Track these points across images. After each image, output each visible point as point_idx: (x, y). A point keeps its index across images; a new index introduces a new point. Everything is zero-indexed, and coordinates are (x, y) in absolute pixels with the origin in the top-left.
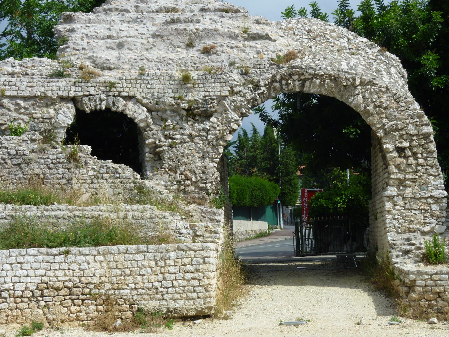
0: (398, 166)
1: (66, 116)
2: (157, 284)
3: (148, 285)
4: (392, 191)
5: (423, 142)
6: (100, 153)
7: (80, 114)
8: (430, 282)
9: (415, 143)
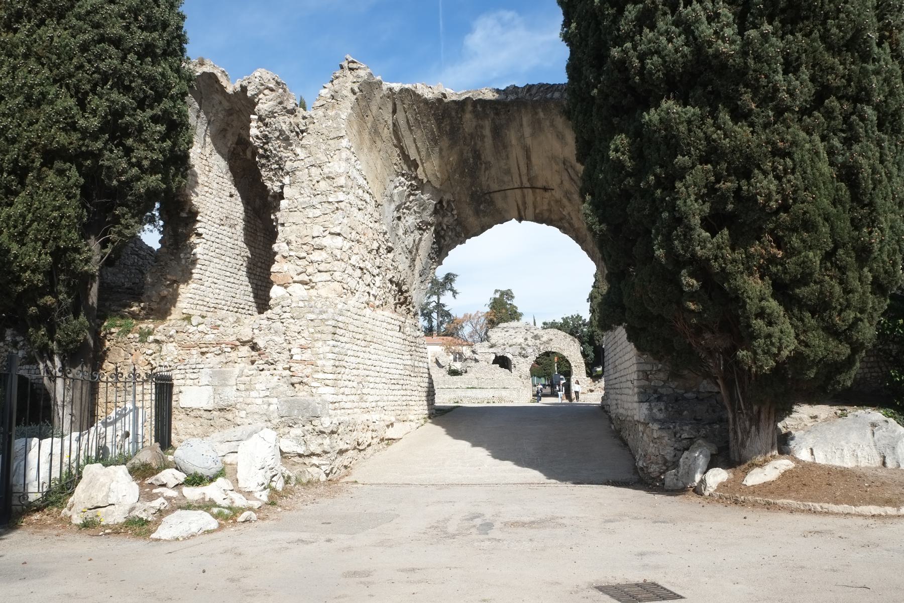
1: (493, 357)
6: (501, 366)
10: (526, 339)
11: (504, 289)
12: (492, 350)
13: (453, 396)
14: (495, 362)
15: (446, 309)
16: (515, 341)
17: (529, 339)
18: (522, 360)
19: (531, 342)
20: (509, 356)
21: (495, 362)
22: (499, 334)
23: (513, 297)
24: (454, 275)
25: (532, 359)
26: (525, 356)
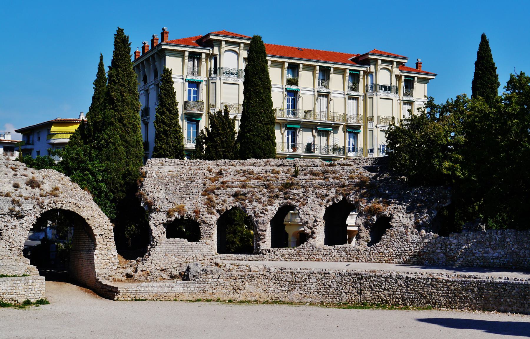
0: (99, 242)
2: (25, 293)
3: (21, 293)
4: (96, 252)
5: (109, 232)
8: (125, 291)
9: (106, 233)
10: (16, 186)
17: (22, 185)
18: (15, 222)
19: (25, 191)
25: (30, 220)
26: (19, 217)
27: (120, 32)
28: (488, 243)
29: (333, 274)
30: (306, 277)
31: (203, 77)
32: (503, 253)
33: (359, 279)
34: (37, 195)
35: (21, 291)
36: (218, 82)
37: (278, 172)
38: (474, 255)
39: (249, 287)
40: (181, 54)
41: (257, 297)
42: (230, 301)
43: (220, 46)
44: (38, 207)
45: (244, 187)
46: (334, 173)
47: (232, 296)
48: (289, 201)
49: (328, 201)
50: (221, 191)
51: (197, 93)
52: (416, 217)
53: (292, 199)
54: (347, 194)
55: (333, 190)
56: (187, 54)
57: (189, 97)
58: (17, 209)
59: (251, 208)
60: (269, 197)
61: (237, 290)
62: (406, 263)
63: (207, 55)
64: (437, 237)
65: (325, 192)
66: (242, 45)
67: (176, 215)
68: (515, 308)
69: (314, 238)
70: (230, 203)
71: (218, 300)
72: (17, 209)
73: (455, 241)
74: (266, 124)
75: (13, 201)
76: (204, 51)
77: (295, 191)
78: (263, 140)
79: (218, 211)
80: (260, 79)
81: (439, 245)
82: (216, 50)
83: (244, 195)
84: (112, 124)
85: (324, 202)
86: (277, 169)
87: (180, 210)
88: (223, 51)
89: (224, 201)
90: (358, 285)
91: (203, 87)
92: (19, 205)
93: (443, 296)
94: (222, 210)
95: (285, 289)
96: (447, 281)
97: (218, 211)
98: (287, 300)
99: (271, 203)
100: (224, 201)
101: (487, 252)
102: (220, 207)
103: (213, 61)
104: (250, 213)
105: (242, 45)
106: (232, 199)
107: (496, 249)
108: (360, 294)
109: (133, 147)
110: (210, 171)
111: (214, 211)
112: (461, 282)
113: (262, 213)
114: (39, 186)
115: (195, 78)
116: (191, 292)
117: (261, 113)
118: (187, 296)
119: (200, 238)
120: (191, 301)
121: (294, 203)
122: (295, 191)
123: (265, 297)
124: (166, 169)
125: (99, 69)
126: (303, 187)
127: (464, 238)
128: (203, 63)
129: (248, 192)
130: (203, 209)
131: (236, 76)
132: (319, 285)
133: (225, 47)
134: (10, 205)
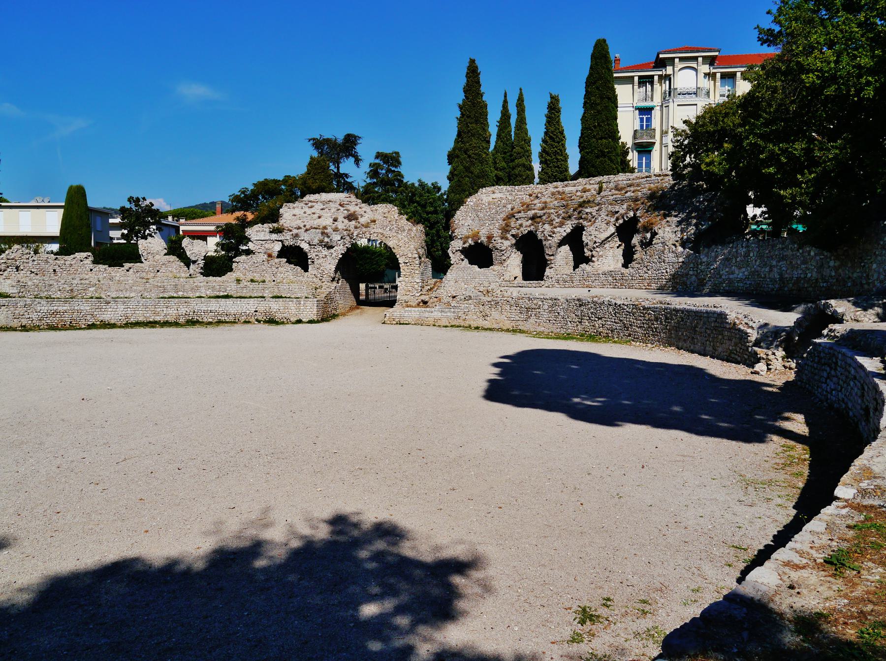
1: (278, 247)
7: (283, 245)
10: (335, 220)
11: (388, 150)
12: (274, 236)
13: (183, 311)
14: (281, 254)
15: (349, 180)
16: (317, 222)
17: (341, 219)
18: (325, 252)
19: (342, 224)
20: (305, 246)
21: (281, 254)
22: (296, 211)
23: (399, 163)
24: (355, 137)
25: (339, 250)
27: (472, 61)
28: (734, 261)
29: (562, 300)
30: (540, 303)
31: (657, 100)
32: (746, 273)
33: (581, 305)
34: (352, 229)
35: (294, 311)
36: (671, 105)
37: (589, 190)
38: (721, 277)
39: (495, 314)
40: (630, 80)
41: (501, 325)
42: (477, 328)
43: (673, 65)
44: (348, 238)
45: (543, 209)
46: (638, 185)
47: (481, 323)
48: (581, 221)
49: (617, 219)
50: (522, 214)
51: (649, 120)
52: (682, 231)
53: (585, 219)
54: (637, 210)
55: (625, 206)
56: (636, 79)
57: (642, 126)
58: (326, 240)
59: (543, 230)
60: (563, 218)
61: (485, 316)
62: (661, 289)
63: (660, 77)
64: (691, 254)
65: (617, 208)
66: (700, 59)
67: (470, 242)
68: (688, 344)
69: (593, 262)
70: (526, 226)
71: (470, 327)
72: (326, 240)
73: (705, 259)
74: (601, 139)
75: (323, 233)
76: (656, 73)
77: (588, 210)
78: (598, 157)
79: (513, 236)
80: (598, 88)
81: (692, 265)
82: (669, 70)
83: (540, 217)
84: (458, 157)
85: (613, 220)
86: (588, 187)
87: (476, 236)
88: (676, 69)
89: (521, 225)
90: (579, 313)
91: (656, 113)
92: (328, 237)
93: (640, 327)
94: (517, 234)
95: (523, 316)
96: (644, 308)
97: (513, 236)
98: (525, 329)
99: (561, 225)
100: (521, 225)
101: (733, 273)
102: (514, 232)
103: (667, 82)
104: (540, 236)
105: (700, 59)
106: (530, 222)
107: (740, 268)
108: (580, 322)
109: (478, 177)
110: (530, 195)
111: (508, 236)
112: (654, 309)
113: (550, 236)
114: (356, 219)
115: (648, 104)
116: (447, 317)
117: (595, 126)
118: (444, 322)
119: (492, 264)
120: (446, 327)
121: (585, 223)
122: (588, 210)
123: (508, 325)
124: (498, 195)
125: (503, 106)
126: (599, 204)
127: (713, 254)
128: (657, 86)
129: (544, 214)
130: (497, 233)
131: (694, 96)
132: (550, 312)
133: (679, 65)
134: (320, 237)
